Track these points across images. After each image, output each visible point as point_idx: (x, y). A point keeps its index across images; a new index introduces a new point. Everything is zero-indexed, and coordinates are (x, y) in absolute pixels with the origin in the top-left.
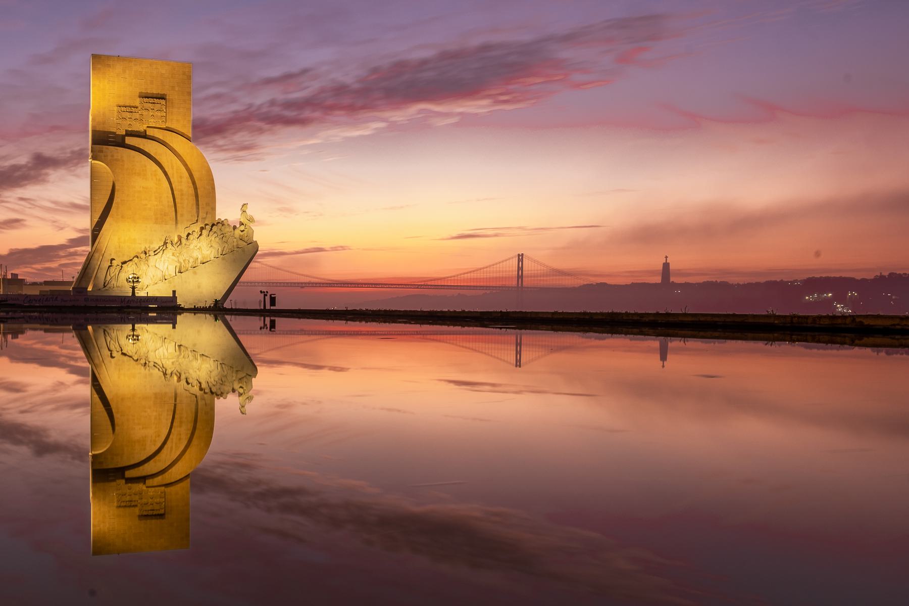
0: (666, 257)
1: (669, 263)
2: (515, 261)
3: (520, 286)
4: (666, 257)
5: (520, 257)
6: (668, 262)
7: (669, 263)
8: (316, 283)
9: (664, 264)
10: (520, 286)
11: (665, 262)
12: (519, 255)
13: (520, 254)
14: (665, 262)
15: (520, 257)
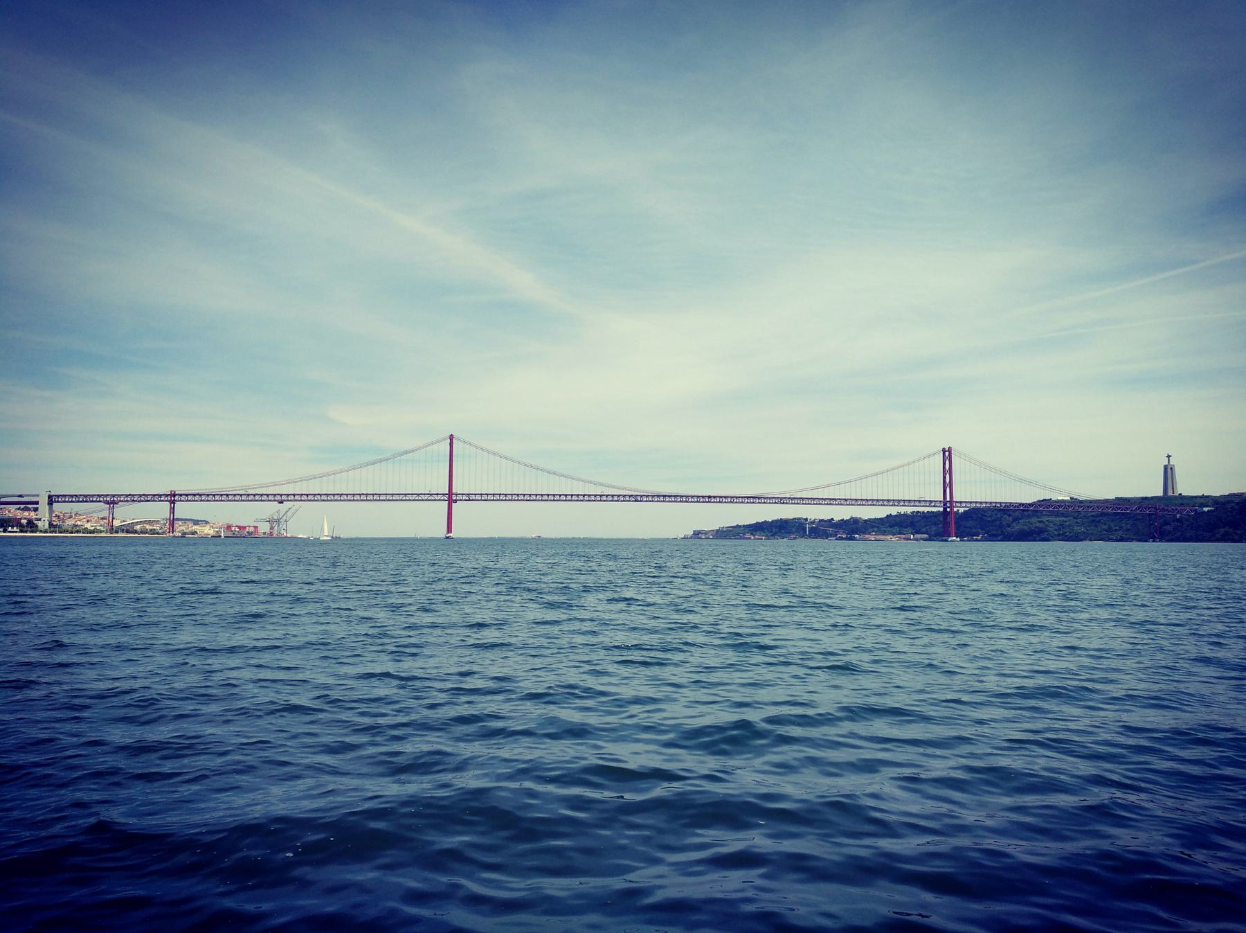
0: (1169, 456)
1: (1174, 465)
2: (939, 458)
3: (948, 499)
4: (1169, 456)
5: (947, 453)
6: (1171, 463)
7: (1174, 465)
8: (613, 496)
9: (1166, 467)
10: (948, 499)
11: (1167, 463)
12: (944, 451)
13: (947, 449)
14: (1167, 463)
15: (947, 453)
